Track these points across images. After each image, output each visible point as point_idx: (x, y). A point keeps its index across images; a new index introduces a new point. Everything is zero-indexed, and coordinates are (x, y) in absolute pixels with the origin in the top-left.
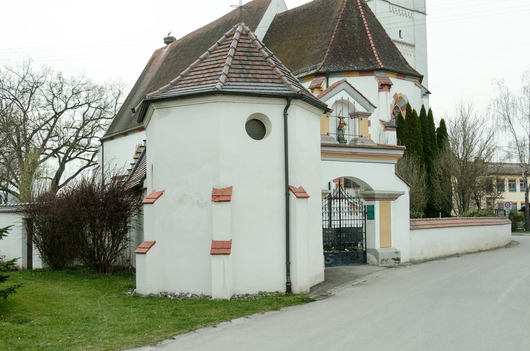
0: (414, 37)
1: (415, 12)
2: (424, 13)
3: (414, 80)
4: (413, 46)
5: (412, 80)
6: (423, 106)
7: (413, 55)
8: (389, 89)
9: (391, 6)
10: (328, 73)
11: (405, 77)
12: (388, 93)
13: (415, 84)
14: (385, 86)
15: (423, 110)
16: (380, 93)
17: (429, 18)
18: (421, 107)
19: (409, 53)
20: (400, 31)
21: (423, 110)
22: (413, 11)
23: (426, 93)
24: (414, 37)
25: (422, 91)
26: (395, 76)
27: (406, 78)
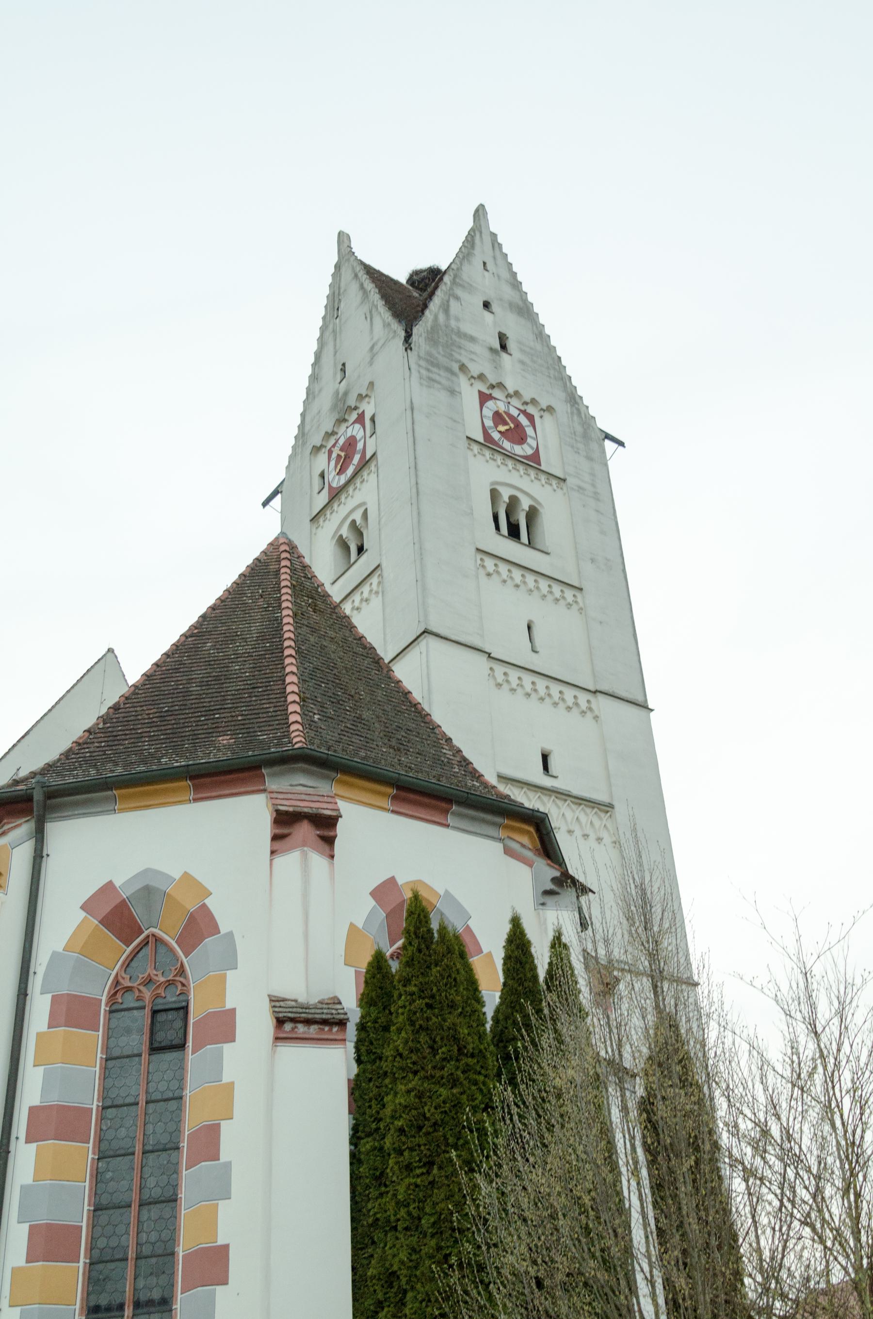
0: (609, 777)
1: (600, 697)
2: (644, 706)
3: (502, 834)
4: (606, 808)
5: (492, 831)
6: (516, 922)
7: (607, 839)
8: (329, 841)
9: (499, 670)
10: (38, 796)
11: (446, 812)
12: (317, 860)
13: (508, 851)
14: (305, 827)
15: (518, 944)
16: (279, 860)
17: (659, 722)
18: (507, 927)
19: (588, 830)
20: (545, 758)
21: (518, 944)
22: (595, 692)
23: (554, 880)
24: (609, 777)
25: (536, 879)
26: (387, 803)
27: (450, 820)
